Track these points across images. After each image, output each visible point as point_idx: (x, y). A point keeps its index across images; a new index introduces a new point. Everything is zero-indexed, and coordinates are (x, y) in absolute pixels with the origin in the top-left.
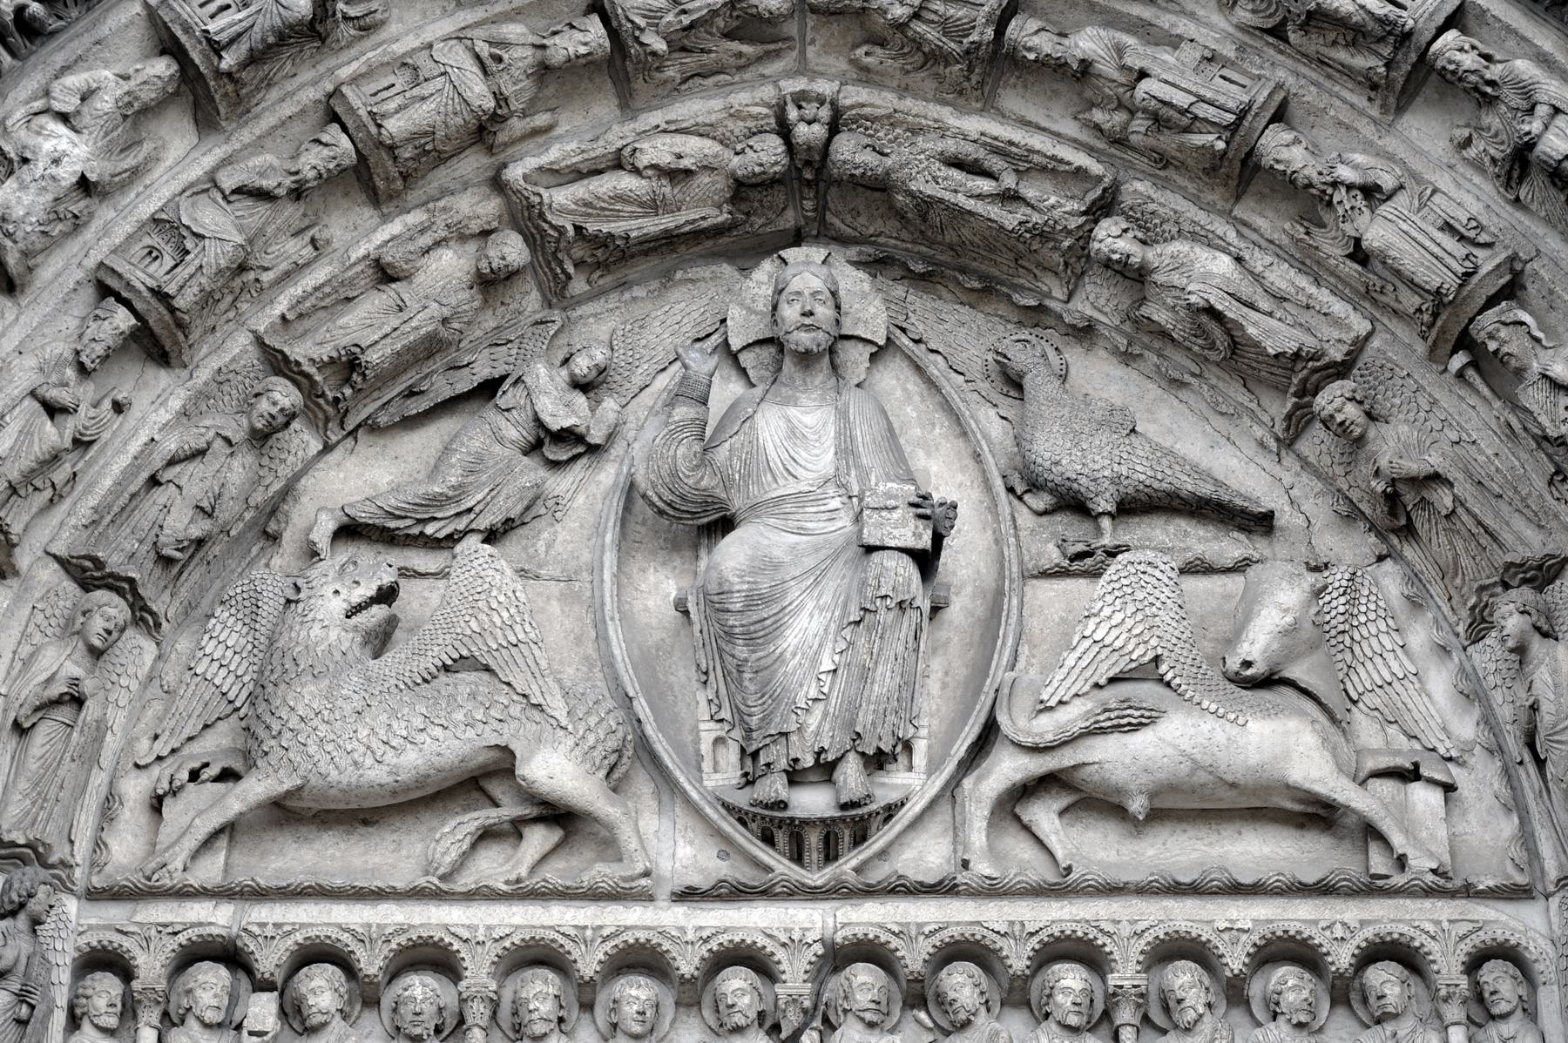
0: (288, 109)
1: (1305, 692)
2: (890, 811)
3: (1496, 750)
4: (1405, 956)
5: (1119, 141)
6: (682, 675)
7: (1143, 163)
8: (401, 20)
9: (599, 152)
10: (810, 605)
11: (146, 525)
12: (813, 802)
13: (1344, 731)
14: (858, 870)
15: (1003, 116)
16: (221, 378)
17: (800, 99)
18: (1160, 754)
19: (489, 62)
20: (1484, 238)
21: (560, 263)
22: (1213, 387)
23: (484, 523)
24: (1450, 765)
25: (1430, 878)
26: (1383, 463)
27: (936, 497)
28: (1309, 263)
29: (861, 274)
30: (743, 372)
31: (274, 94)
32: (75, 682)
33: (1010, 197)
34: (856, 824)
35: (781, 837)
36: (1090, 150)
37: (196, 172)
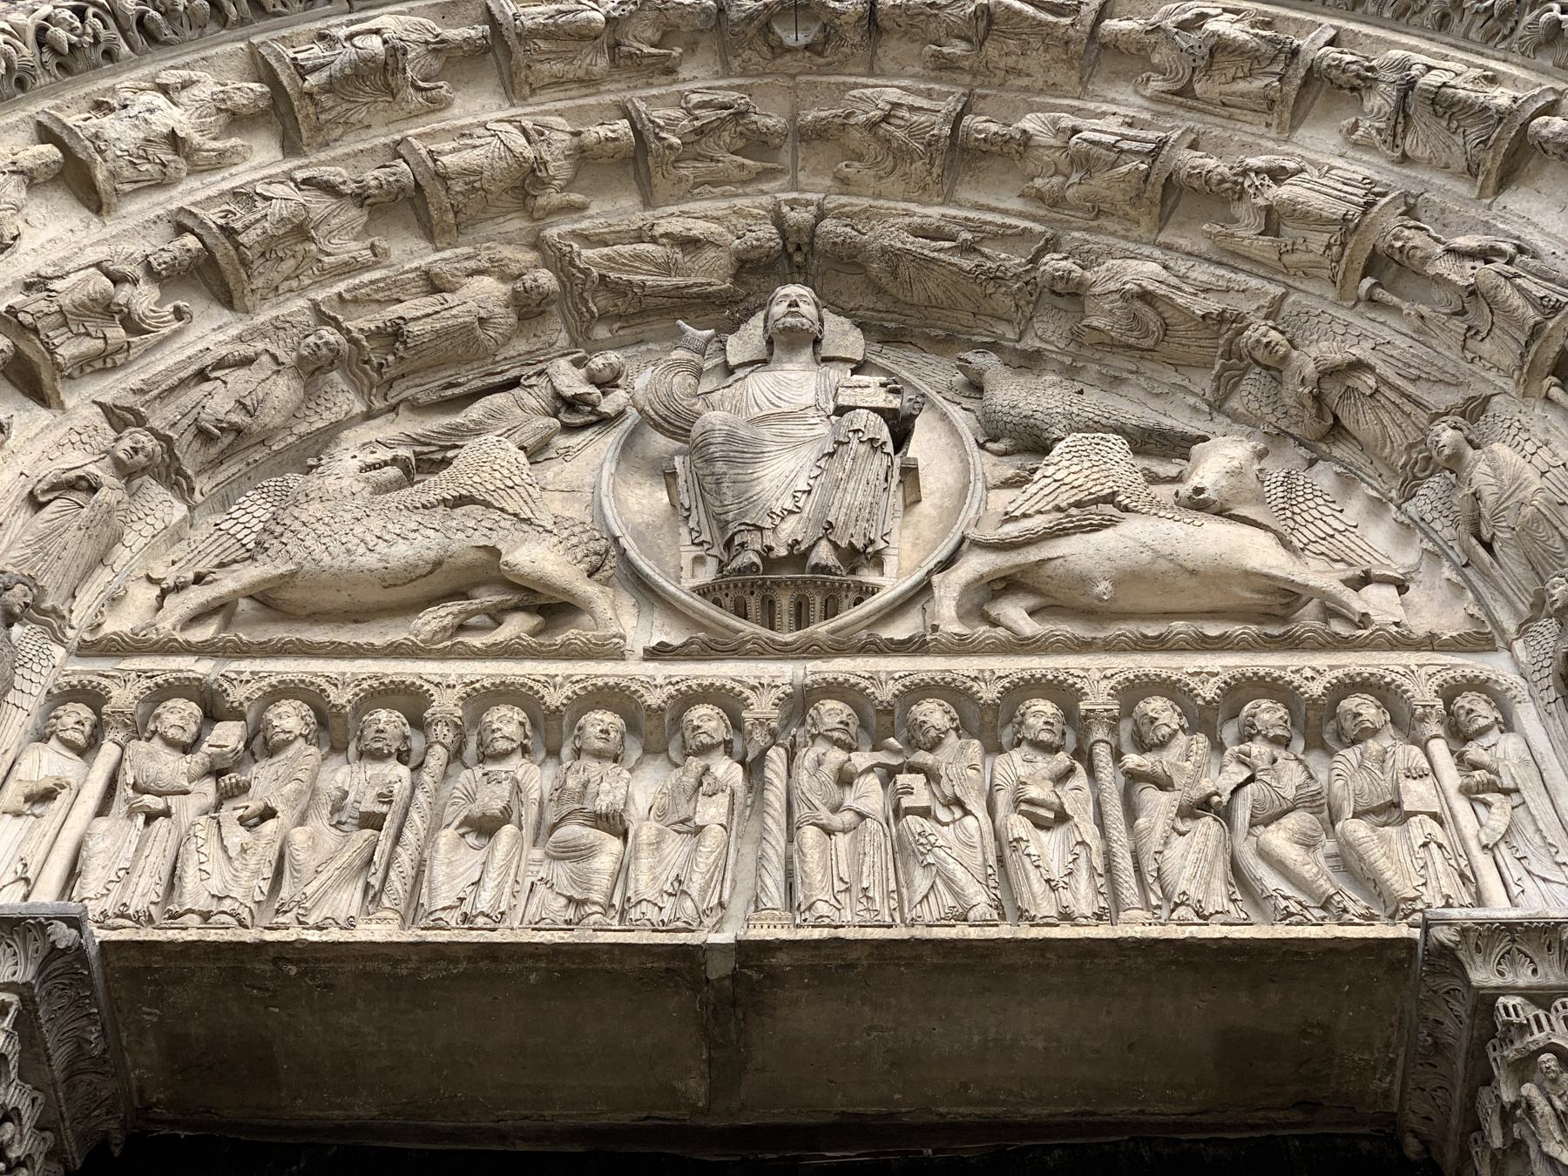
5: (1056, 202)
8: (463, 107)
15: (960, 206)
17: (793, 204)
18: (1121, 545)
28: (1231, 257)
33: (968, 249)
35: (753, 604)
36: (1034, 219)
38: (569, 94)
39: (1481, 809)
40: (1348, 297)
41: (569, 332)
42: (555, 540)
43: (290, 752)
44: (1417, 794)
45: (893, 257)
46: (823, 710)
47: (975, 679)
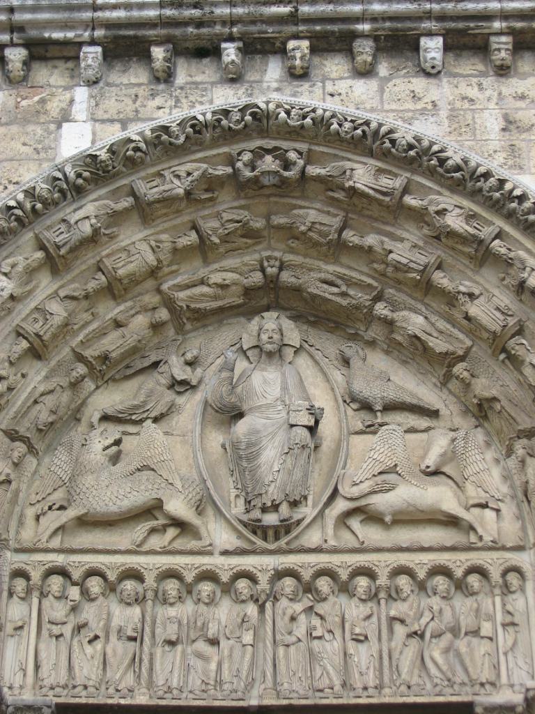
0: (84, 267)
1: (449, 477)
2: (299, 522)
3: (514, 497)
4: (481, 572)
6: (223, 471)
7: (391, 282)
9: (195, 279)
10: (270, 447)
11: (33, 417)
12: (271, 519)
13: (462, 491)
14: (287, 544)
15: (342, 265)
16: (59, 364)
17: (268, 258)
19: (155, 248)
20: (510, 313)
21: (181, 319)
22: (418, 363)
23: (153, 415)
24: (500, 503)
25: (490, 544)
26: (477, 393)
27: (317, 406)
29: (291, 322)
30: (248, 358)
31: (79, 262)
32: (8, 475)
33: (344, 295)
34: (286, 527)
35: (259, 532)
36: (373, 278)
37: (50, 291)
38: (169, 218)
39: (506, 633)
40: (495, 355)
43: (98, 603)
44: (486, 628)
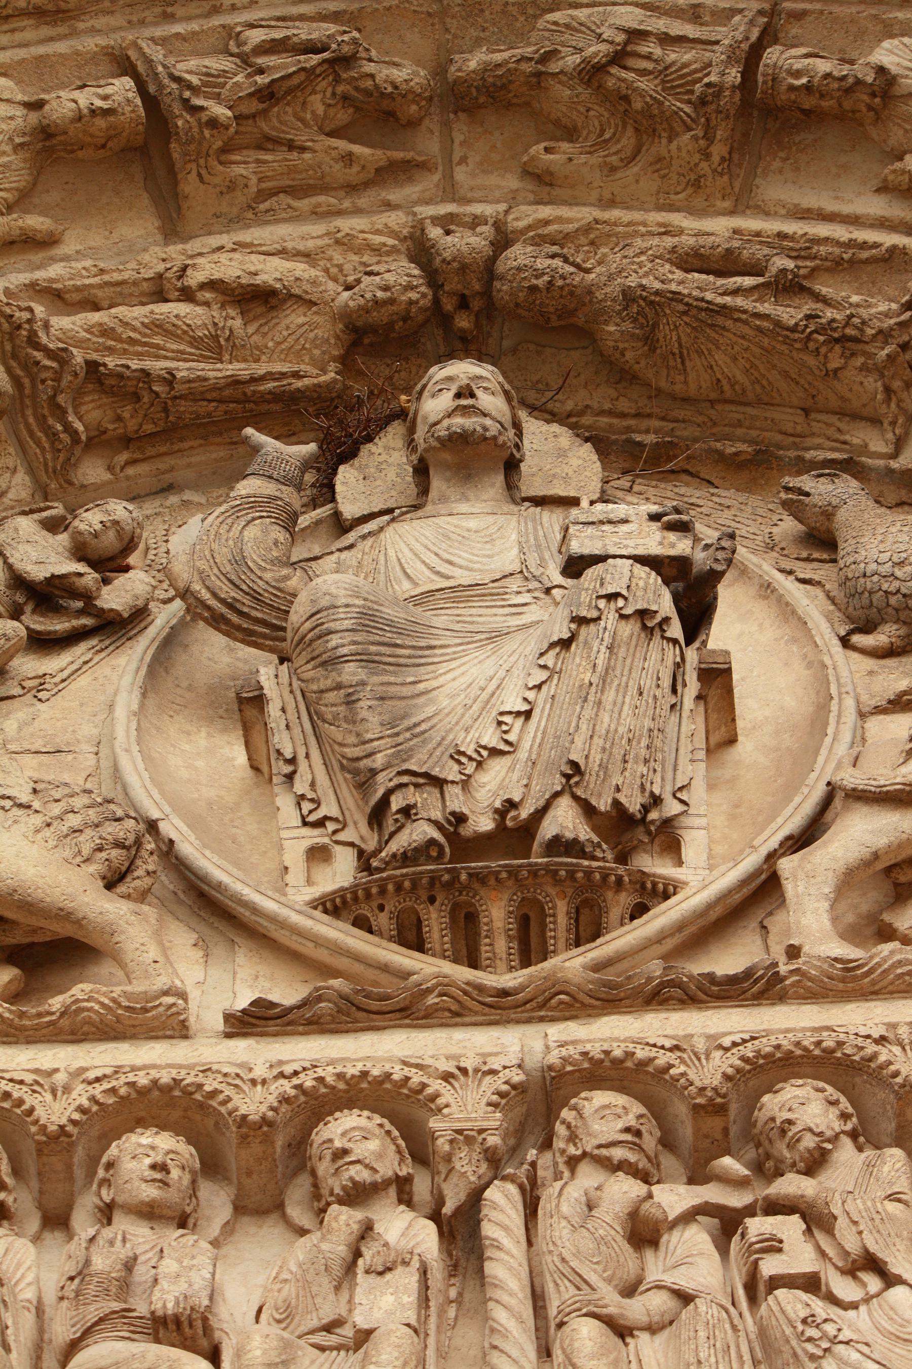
17: (447, 223)
33: (788, 287)
35: (435, 922)
38: (18, 37)
41: (31, 471)
42: (38, 820)
45: (646, 307)
46: (588, 1109)
47: (882, 1040)
